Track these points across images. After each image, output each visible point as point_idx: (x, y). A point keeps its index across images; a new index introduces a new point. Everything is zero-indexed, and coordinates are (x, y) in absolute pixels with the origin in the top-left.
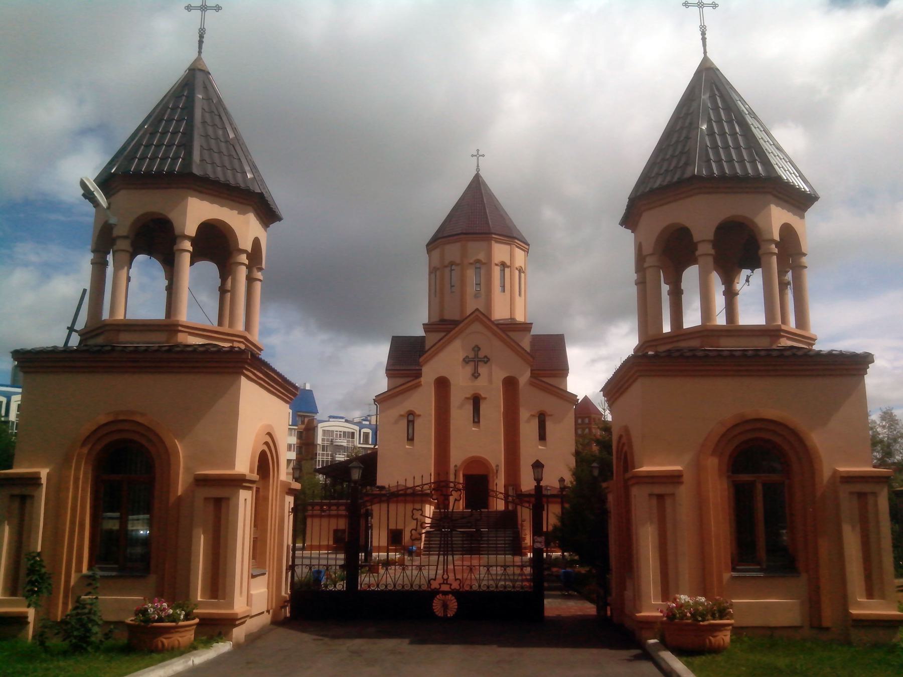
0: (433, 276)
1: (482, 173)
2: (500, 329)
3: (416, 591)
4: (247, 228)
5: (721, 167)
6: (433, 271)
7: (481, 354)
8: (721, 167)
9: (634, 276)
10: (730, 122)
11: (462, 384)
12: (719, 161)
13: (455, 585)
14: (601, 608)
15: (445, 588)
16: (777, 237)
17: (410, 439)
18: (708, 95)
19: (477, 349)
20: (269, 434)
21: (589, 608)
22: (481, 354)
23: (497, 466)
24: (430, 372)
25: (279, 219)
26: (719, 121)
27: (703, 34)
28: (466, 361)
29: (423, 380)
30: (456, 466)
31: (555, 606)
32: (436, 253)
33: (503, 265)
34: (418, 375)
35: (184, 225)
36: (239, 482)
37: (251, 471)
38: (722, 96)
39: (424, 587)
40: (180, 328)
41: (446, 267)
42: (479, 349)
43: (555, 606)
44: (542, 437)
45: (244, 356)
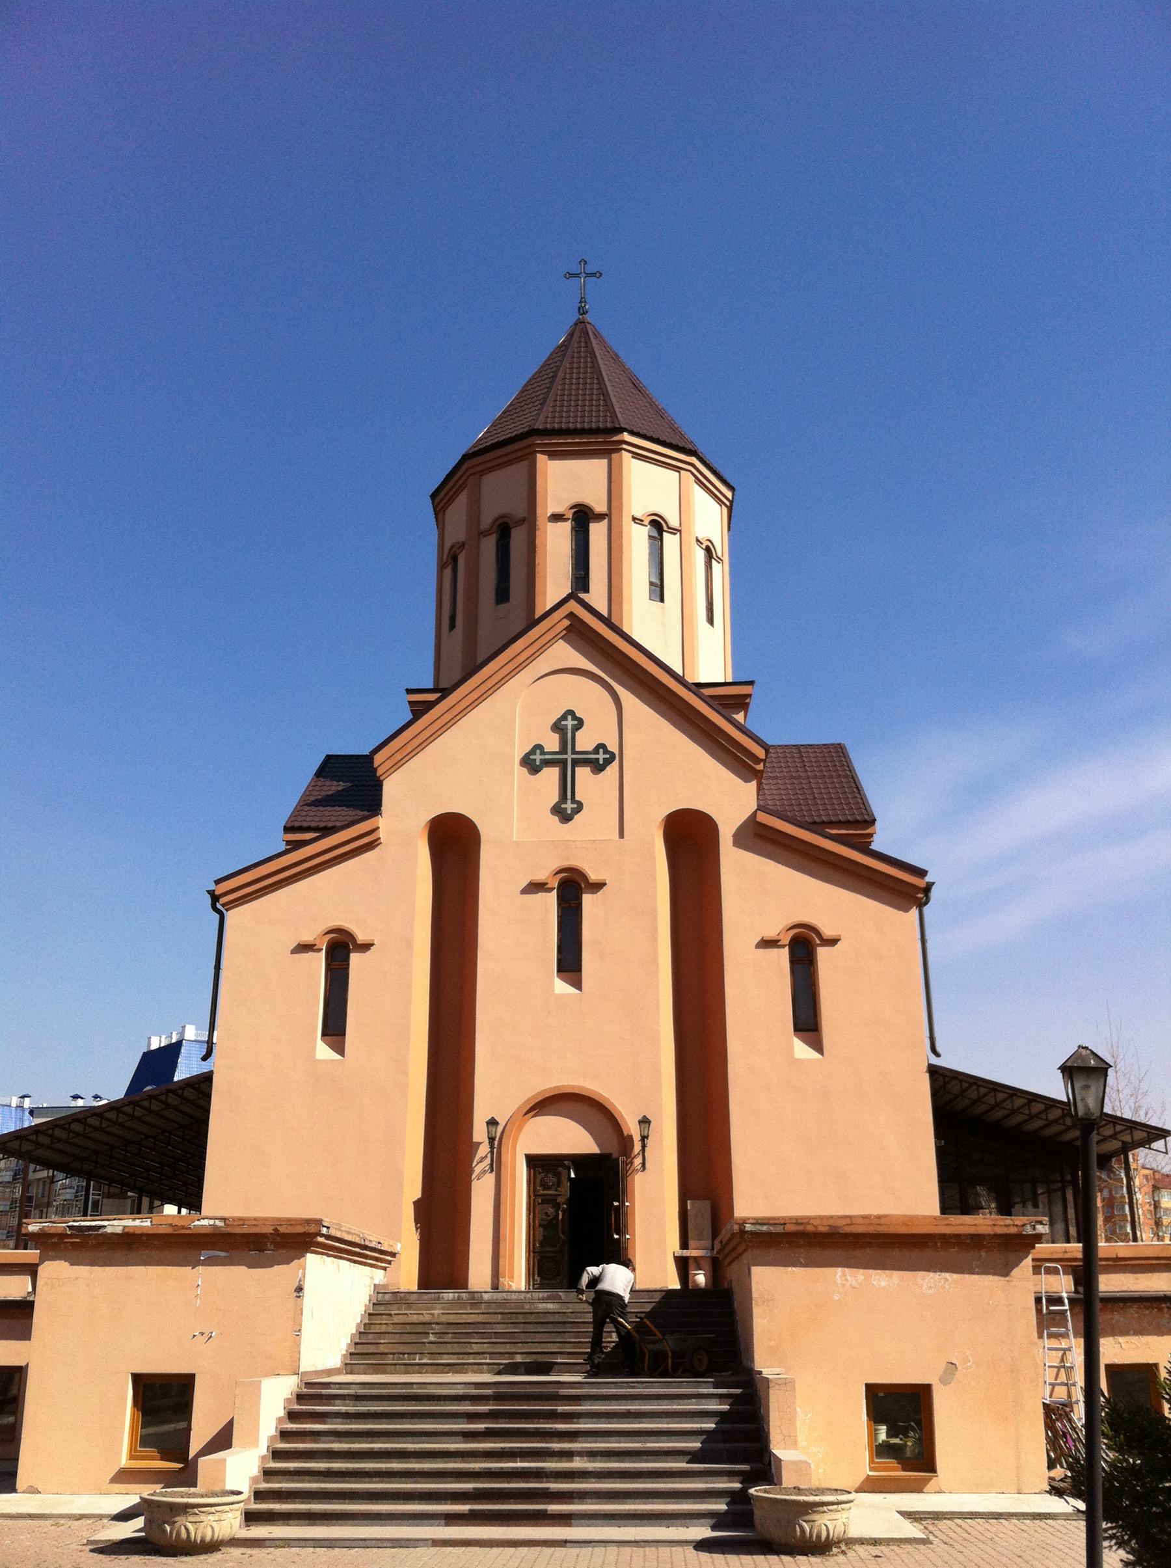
0: (448, 572)
7: (585, 741)
11: (519, 842)
17: (334, 1027)
19: (567, 725)
22: (585, 741)
23: (645, 1122)
28: (532, 763)
29: (385, 823)
30: (492, 1123)
33: (658, 526)
41: (485, 533)
42: (580, 723)
44: (807, 1021)
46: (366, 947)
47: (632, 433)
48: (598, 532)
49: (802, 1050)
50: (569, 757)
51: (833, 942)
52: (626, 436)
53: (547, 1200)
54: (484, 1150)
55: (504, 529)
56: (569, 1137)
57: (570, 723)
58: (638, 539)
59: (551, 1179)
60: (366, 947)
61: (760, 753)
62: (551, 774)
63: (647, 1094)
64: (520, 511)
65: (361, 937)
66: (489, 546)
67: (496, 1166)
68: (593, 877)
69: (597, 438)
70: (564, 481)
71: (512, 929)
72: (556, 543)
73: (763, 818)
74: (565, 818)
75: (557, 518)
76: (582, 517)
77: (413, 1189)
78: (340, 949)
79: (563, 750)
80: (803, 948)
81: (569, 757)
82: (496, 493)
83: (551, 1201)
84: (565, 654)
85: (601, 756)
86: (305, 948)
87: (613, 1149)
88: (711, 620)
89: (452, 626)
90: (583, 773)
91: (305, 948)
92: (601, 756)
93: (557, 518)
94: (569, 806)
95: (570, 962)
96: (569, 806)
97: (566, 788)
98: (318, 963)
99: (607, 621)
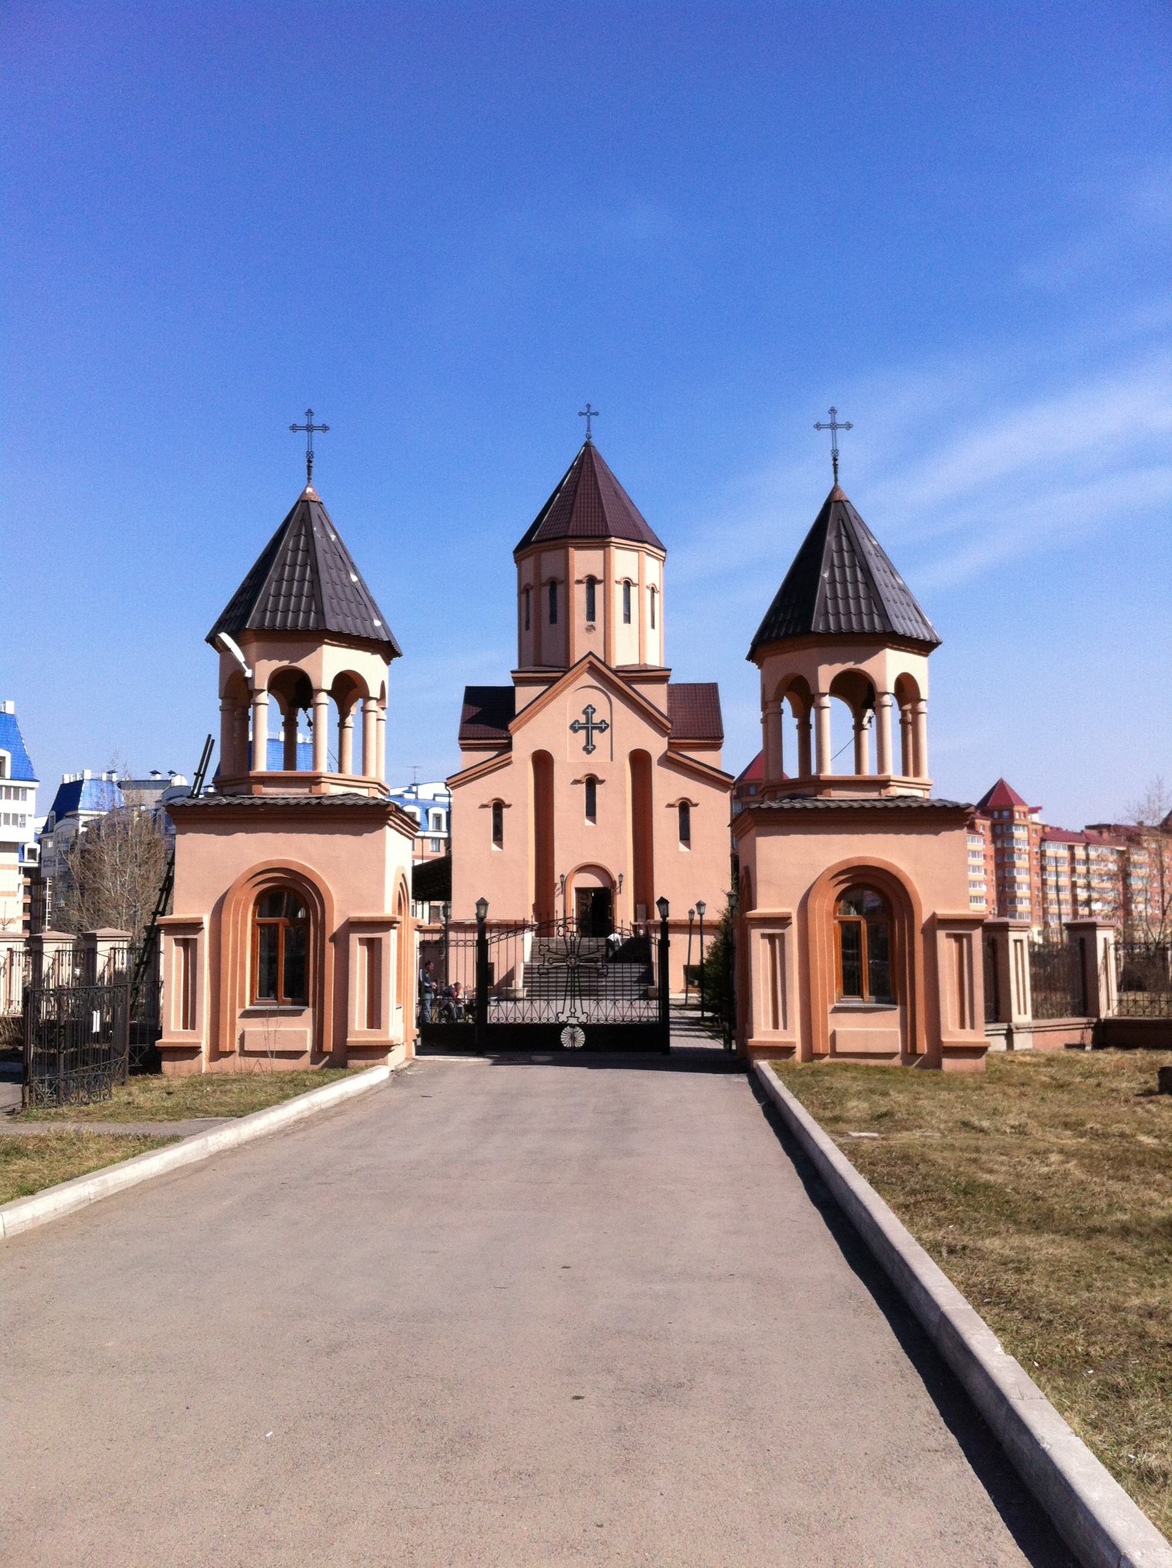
0: (524, 596)
1: (594, 442)
2: (621, 678)
4: (369, 667)
6: (524, 591)
7: (596, 719)
9: (760, 715)
10: (853, 567)
13: (583, 1019)
14: (727, 1042)
15: (573, 1021)
16: (891, 688)
18: (834, 534)
19: (589, 711)
21: (718, 1044)
22: (596, 719)
23: (621, 876)
24: (526, 739)
25: (399, 655)
27: (835, 460)
28: (575, 728)
29: (514, 754)
30: (562, 876)
32: (529, 563)
33: (628, 584)
34: (508, 747)
35: (320, 679)
36: (386, 925)
37: (394, 912)
38: (848, 537)
39: (552, 1021)
41: (545, 585)
43: (678, 1040)
44: (685, 835)
45: (389, 809)
48: (599, 589)
49: (682, 848)
51: (696, 805)
52: (613, 539)
53: (583, 904)
54: (559, 886)
55: (553, 584)
58: (618, 591)
60: (509, 806)
61: (669, 725)
62: (583, 733)
63: (623, 866)
64: (561, 577)
65: (507, 802)
66: (546, 591)
67: (564, 892)
68: (600, 778)
69: (599, 539)
70: (583, 562)
71: (568, 800)
72: (579, 594)
73: (669, 754)
74: (589, 752)
75: (579, 582)
76: (591, 581)
77: (532, 900)
78: (498, 807)
80: (685, 807)
86: (484, 806)
87: (609, 885)
88: (653, 627)
89: (527, 628)
90: (596, 732)
91: (484, 806)
92: (603, 726)
93: (579, 582)
94: (590, 747)
95: (591, 812)
96: (590, 747)
97: (589, 739)
98: (490, 812)
99: (604, 664)
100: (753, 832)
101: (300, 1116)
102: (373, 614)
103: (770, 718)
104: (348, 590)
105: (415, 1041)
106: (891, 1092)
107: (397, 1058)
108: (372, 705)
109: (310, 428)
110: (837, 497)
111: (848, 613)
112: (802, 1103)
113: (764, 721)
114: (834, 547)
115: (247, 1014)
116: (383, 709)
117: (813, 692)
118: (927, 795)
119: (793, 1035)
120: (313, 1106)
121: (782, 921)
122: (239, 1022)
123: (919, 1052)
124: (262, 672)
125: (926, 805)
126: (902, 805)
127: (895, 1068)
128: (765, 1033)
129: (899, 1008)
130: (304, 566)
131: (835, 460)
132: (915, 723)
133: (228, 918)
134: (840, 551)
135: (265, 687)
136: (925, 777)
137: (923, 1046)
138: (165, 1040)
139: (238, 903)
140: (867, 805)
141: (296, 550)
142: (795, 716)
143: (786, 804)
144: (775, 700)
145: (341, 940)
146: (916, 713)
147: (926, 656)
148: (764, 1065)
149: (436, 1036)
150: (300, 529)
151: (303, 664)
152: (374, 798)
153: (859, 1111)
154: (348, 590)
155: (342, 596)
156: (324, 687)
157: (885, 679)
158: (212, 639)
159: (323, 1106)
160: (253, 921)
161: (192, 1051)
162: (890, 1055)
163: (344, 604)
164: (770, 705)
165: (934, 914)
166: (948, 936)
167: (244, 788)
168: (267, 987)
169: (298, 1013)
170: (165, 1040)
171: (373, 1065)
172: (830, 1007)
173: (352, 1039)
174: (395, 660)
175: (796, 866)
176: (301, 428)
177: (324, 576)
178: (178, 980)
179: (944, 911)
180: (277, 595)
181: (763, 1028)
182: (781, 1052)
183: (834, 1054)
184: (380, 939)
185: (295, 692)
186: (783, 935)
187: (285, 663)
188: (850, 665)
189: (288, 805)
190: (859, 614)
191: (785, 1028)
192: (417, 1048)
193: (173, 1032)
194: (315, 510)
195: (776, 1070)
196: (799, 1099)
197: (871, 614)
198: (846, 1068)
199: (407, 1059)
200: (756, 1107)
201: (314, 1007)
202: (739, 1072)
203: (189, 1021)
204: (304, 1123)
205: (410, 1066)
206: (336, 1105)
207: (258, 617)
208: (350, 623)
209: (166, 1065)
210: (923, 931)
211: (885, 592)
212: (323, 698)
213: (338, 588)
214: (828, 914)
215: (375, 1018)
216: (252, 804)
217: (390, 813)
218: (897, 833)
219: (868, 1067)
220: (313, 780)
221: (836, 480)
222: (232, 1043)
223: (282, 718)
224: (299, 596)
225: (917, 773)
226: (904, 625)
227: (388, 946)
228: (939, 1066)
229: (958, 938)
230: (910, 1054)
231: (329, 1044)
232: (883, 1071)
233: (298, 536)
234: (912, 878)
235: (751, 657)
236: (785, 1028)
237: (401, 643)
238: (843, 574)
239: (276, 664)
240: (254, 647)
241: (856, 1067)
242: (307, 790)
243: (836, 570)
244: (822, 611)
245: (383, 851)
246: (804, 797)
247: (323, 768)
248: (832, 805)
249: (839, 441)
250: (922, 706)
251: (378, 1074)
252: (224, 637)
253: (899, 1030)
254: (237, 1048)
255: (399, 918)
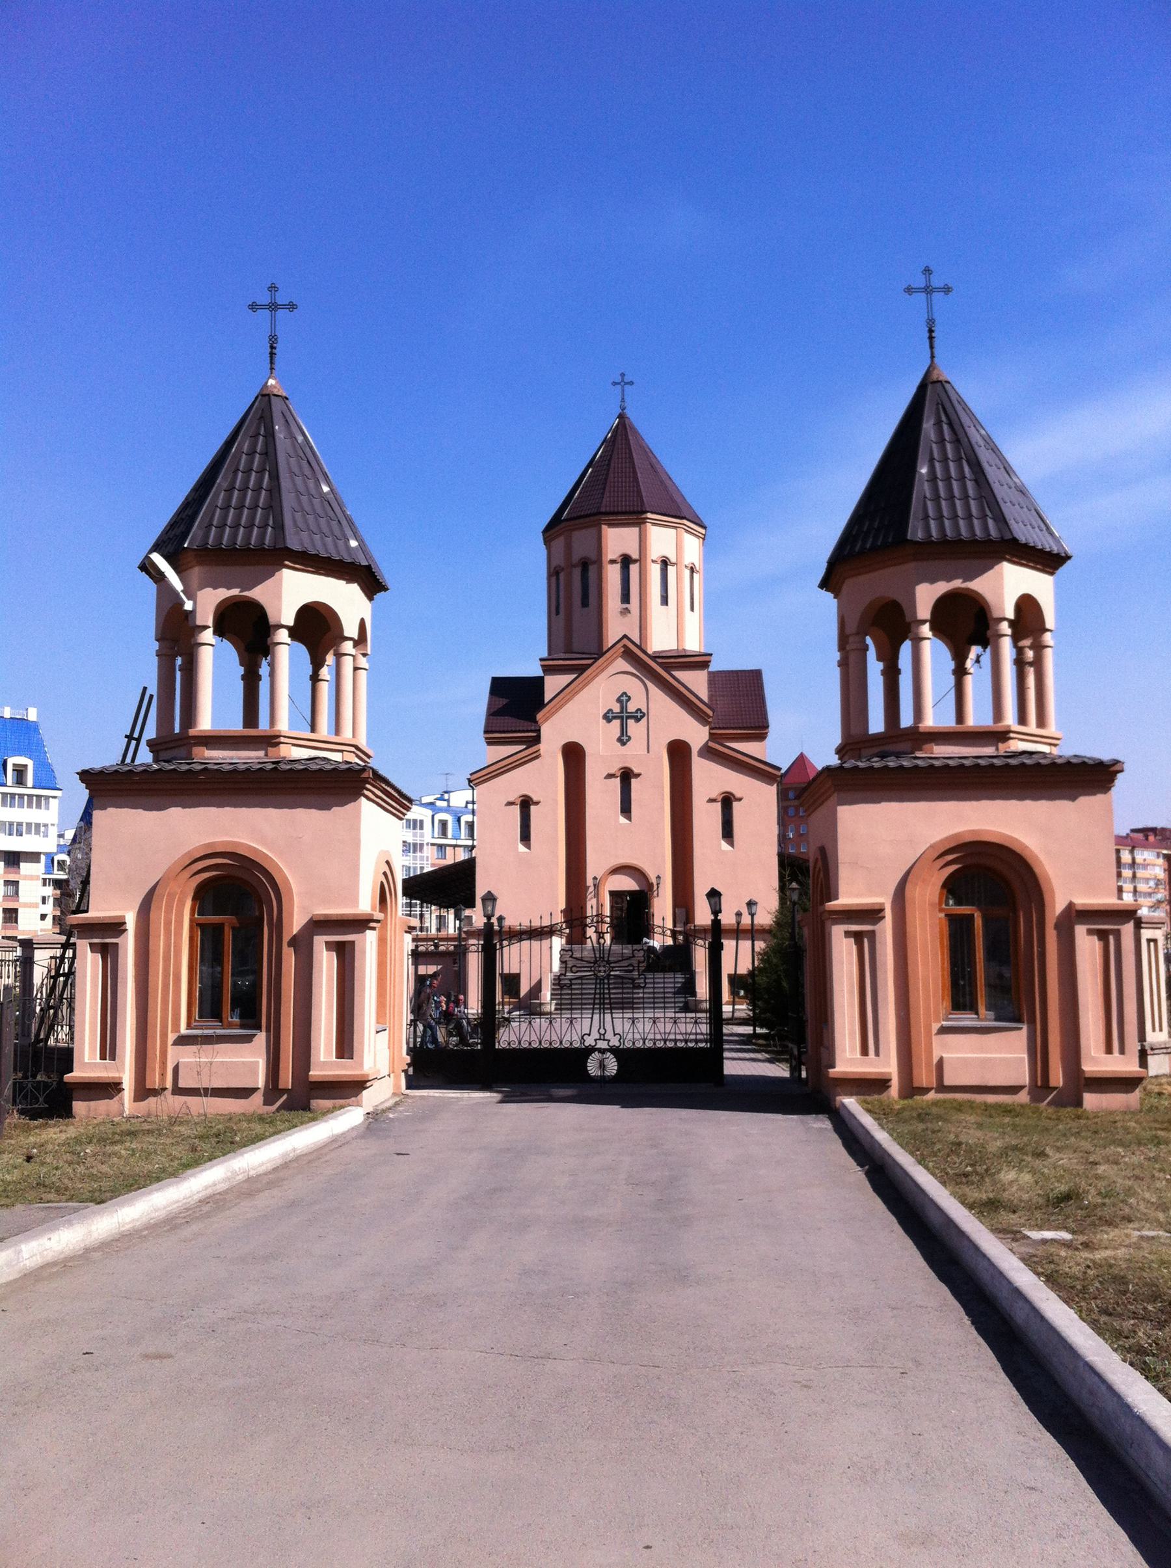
0: (554, 579)
1: (629, 413)
2: (659, 664)
3: (566, 1048)
4: (346, 601)
5: (941, 527)
6: (554, 573)
7: (632, 707)
8: (941, 527)
9: (837, 656)
10: (958, 460)
12: (940, 518)
13: (615, 1042)
14: (795, 1070)
15: (602, 1045)
16: (1010, 614)
17: (525, 837)
18: (932, 422)
19: (623, 699)
20: (387, 862)
21: (780, 1071)
23: (658, 877)
24: (555, 731)
25: (384, 588)
26: (945, 460)
27: (931, 331)
28: (608, 717)
29: (543, 747)
30: (595, 878)
31: (735, 1066)
33: (665, 563)
34: (537, 740)
35: (279, 611)
36: (361, 924)
37: (373, 908)
38: (950, 424)
39: (577, 1045)
40: (282, 739)
41: (575, 566)
42: (629, 698)
43: (735, 1066)
44: (728, 832)
45: (365, 775)
46: (537, 803)
47: (652, 513)
48: (634, 569)
49: (725, 846)
50: (625, 715)
52: (649, 515)
53: (617, 909)
54: (591, 889)
55: (585, 565)
56: (627, 884)
57: (624, 698)
58: (655, 571)
59: (619, 900)
61: (710, 713)
63: (661, 868)
64: (593, 557)
65: (535, 799)
66: (577, 573)
67: (597, 895)
69: (634, 516)
70: (617, 540)
71: (601, 795)
72: (613, 574)
73: (711, 744)
74: (623, 744)
75: (613, 562)
76: (626, 561)
77: (562, 905)
78: (526, 804)
79: (622, 712)
80: (727, 802)
81: (625, 715)
82: (581, 542)
83: (621, 909)
84: (621, 664)
85: (639, 715)
86: (510, 804)
87: (646, 889)
88: (692, 609)
89: (558, 613)
90: (631, 722)
91: (510, 804)
92: (639, 715)
93: (613, 562)
94: (625, 738)
95: (626, 809)
96: (625, 738)
97: (623, 729)
98: (517, 810)
99: (639, 647)
100: (835, 797)
101: (209, 1191)
102: (349, 532)
103: (853, 658)
104: (316, 502)
105: (405, 1071)
106: (1048, 1150)
107: (375, 1097)
108: (348, 647)
109: (273, 307)
110: (934, 377)
111: (955, 517)
112: (933, 1174)
113: (843, 664)
114: (933, 437)
115: (182, 1041)
116: (364, 655)
117: (908, 619)
118: (1055, 751)
119: (887, 1064)
120: (235, 1174)
121: (873, 914)
122: (171, 1050)
123: (1052, 1084)
124: (205, 604)
125: (1059, 761)
126: (1028, 762)
127: (1022, 1106)
128: (851, 1061)
129: (1025, 1027)
130: (261, 472)
131: (931, 331)
132: (1038, 663)
133: (159, 916)
134: (941, 441)
135: (210, 623)
136: (1052, 729)
137: (1057, 1077)
138: (78, 1073)
139: (171, 897)
140: (982, 762)
141: (252, 453)
142: (879, 659)
143: (877, 763)
144: (858, 633)
145: (303, 944)
146: (1039, 648)
147: (1052, 574)
148: (850, 1102)
149: (429, 1066)
150: (258, 428)
151: (257, 593)
152: (347, 762)
153: (1021, 1189)
154: (316, 502)
155: (307, 508)
156: (284, 622)
157: (1003, 602)
158: (147, 567)
159: (252, 1173)
160: (192, 921)
161: (111, 1089)
162: (1014, 1090)
163: (311, 518)
164: (851, 639)
165: (1071, 905)
166: (1090, 932)
167: (182, 752)
168: (209, 1004)
169: (248, 1039)
170: (78, 1073)
171: (342, 1107)
172: (935, 1027)
173: (315, 1073)
174: (379, 596)
175: (886, 846)
176: (262, 307)
177: (285, 483)
178: (94, 996)
179: (1083, 900)
180: (226, 508)
181: (848, 1055)
182: (872, 1086)
183: (942, 1088)
184: (353, 943)
185: (248, 629)
186: (873, 932)
187: (235, 592)
188: (957, 583)
189: (235, 771)
190: (969, 517)
191: (877, 1054)
192: (408, 1077)
193: (88, 1063)
194: (277, 405)
195: (869, 1111)
196: (926, 1168)
197: (983, 517)
198: (959, 1107)
199: (394, 1094)
200: (856, 1175)
201: (268, 1031)
202: (817, 1112)
203: (108, 1049)
204: (214, 1202)
205: (397, 1104)
206: (275, 1170)
207: (201, 533)
208: (318, 544)
209: (79, 1107)
210: (1057, 926)
211: (1001, 492)
212: (283, 636)
213: (304, 499)
214: (931, 905)
215: (345, 1046)
216: (189, 771)
217: (366, 781)
218: (1021, 798)
219: (987, 1107)
220: (271, 741)
221: (933, 357)
222: (163, 1075)
223: (241, 670)
224: (254, 508)
225: (1041, 722)
226: (1024, 533)
227: (364, 952)
228: (1079, 1103)
229: (1103, 935)
230: (1040, 1086)
231: (287, 1079)
232: (1007, 1110)
233: (256, 436)
234: (1042, 857)
235: (825, 584)
236: (877, 1054)
237: (386, 571)
238: (946, 469)
239: (223, 594)
240: (196, 572)
241: (971, 1105)
242: (261, 753)
243: (937, 465)
244: (921, 516)
245: (358, 830)
246: (898, 755)
247: (283, 725)
248: (937, 763)
249: (935, 308)
250: (1048, 638)
251: (348, 1119)
252: (157, 558)
253: (1026, 1056)
254: (169, 1084)
255: (378, 915)
